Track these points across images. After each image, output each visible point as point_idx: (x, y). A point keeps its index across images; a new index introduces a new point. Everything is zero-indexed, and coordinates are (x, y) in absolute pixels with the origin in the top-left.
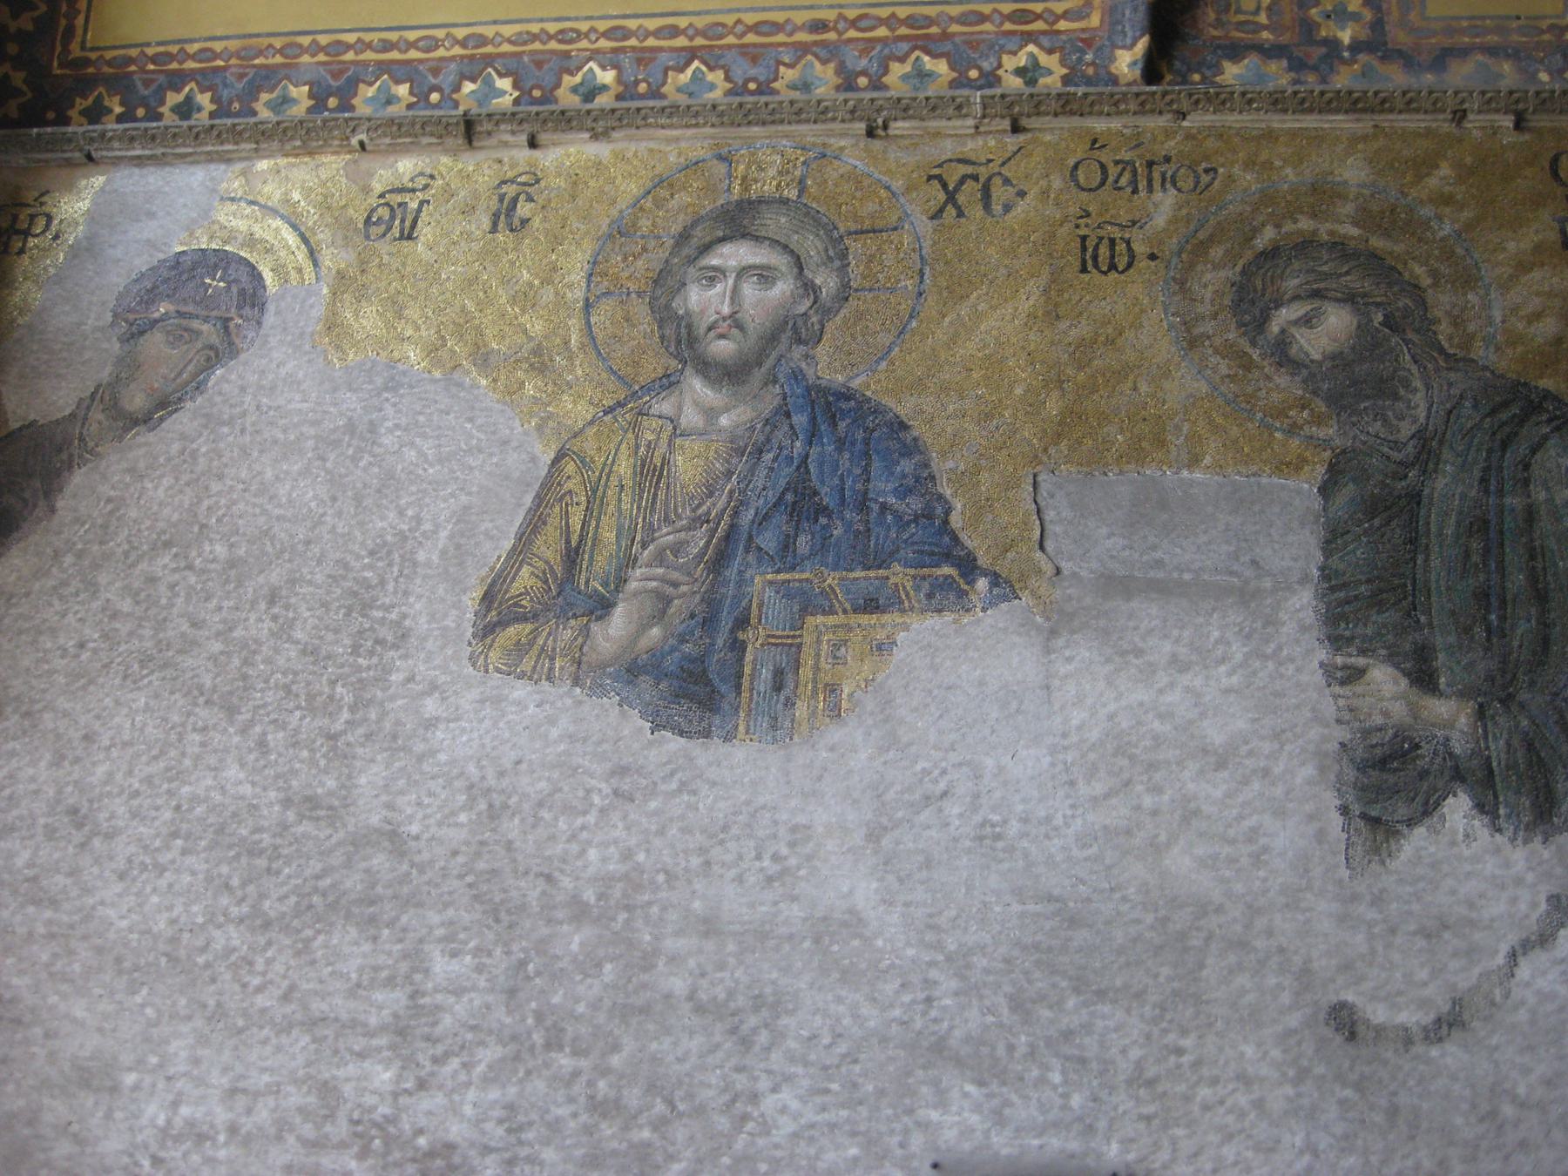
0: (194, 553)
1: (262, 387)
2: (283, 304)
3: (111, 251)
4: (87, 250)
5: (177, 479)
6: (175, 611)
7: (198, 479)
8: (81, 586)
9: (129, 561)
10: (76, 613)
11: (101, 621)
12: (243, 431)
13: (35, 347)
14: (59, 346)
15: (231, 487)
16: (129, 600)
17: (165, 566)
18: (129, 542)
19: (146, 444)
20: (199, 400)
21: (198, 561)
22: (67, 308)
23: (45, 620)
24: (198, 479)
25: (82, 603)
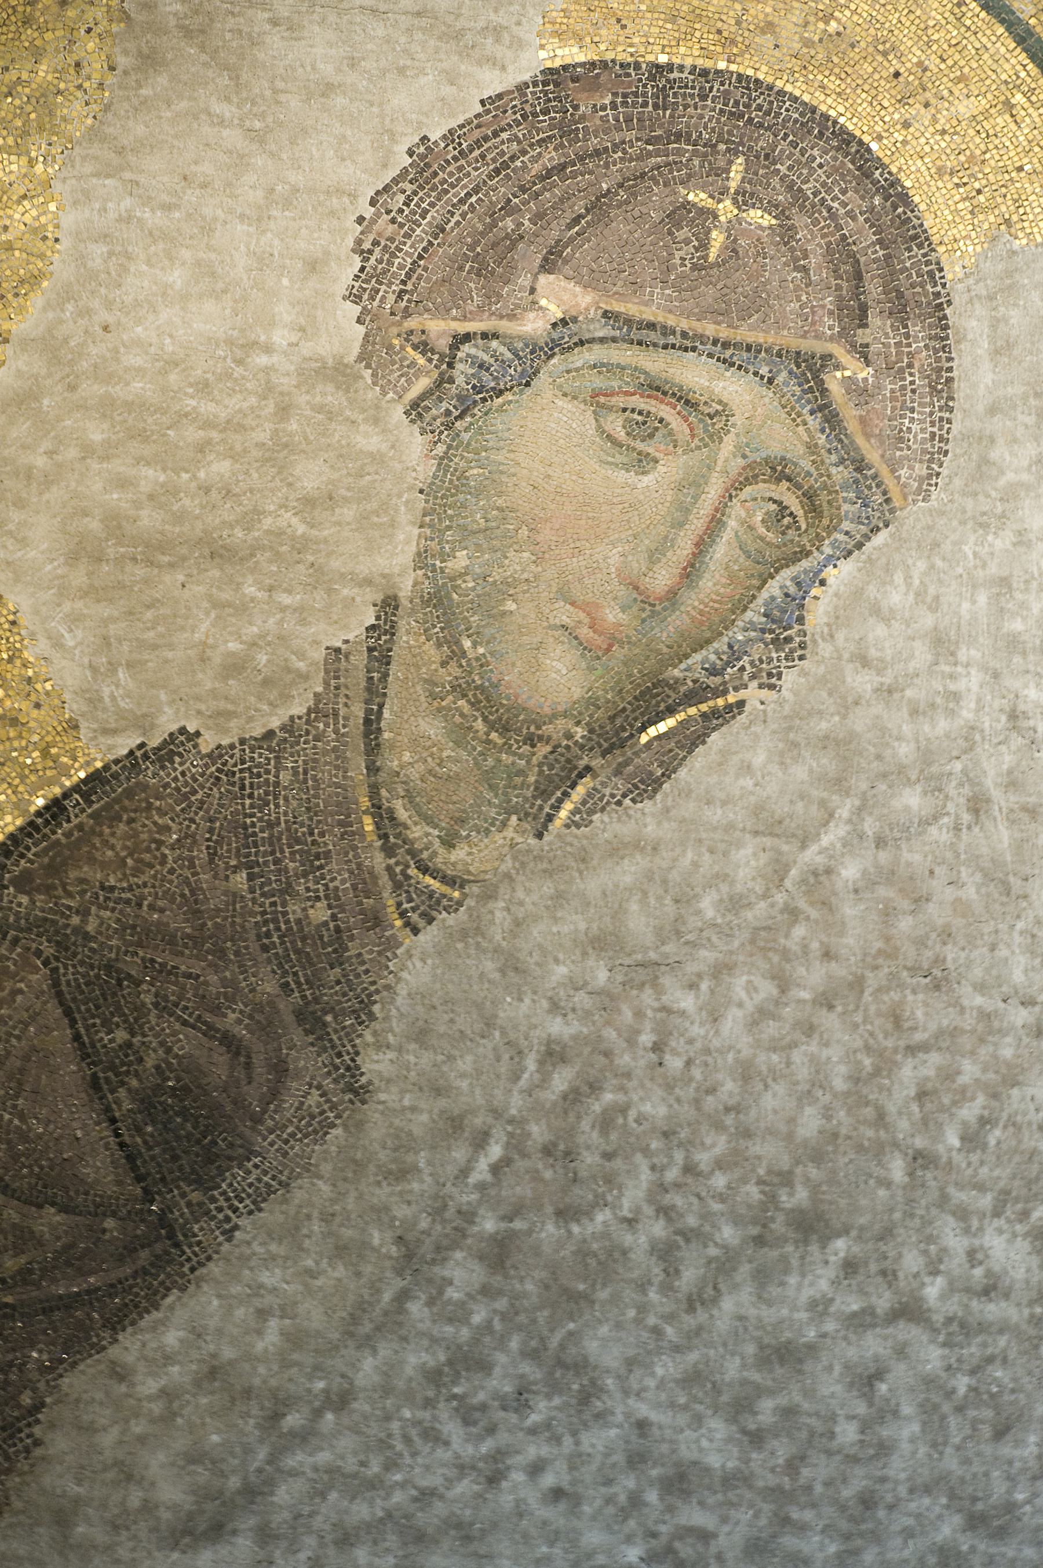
0: (912, 1261)
1: (1014, 644)
2: (1015, 316)
3: (275, 41)
4: (188, 33)
5: (784, 983)
6: (897, 1467)
7: (858, 984)
8: (526, 1368)
9: (689, 1276)
10: (536, 1469)
11: (636, 1501)
12: (978, 805)
13: (96, 433)
14: (193, 434)
15: (985, 1016)
16: (718, 1427)
17: (819, 1307)
18: (665, 1212)
19: (637, 845)
20: (789, 678)
21: (933, 1290)
22: (177, 277)
23: (426, 1496)
24: (858, 984)
25: (545, 1430)
